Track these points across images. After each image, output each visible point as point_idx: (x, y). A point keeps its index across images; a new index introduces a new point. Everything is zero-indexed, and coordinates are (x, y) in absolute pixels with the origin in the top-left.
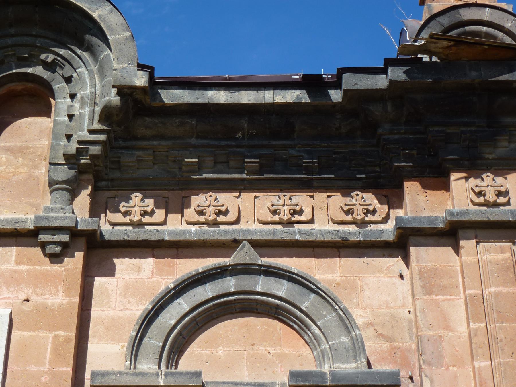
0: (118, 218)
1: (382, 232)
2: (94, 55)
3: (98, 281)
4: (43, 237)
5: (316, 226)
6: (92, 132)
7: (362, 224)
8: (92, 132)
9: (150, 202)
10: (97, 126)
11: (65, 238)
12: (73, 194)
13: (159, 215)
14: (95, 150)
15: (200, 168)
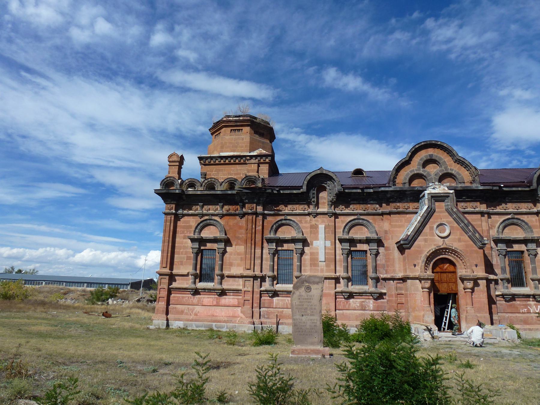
0: (338, 209)
1: (379, 212)
2: (334, 183)
3: (336, 219)
4: (328, 214)
5: (369, 211)
6: (334, 197)
7: (376, 210)
8: (334, 197)
9: (343, 207)
10: (335, 196)
11: (331, 214)
12: (331, 206)
13: (344, 209)
14: (335, 200)
15: (351, 201)
